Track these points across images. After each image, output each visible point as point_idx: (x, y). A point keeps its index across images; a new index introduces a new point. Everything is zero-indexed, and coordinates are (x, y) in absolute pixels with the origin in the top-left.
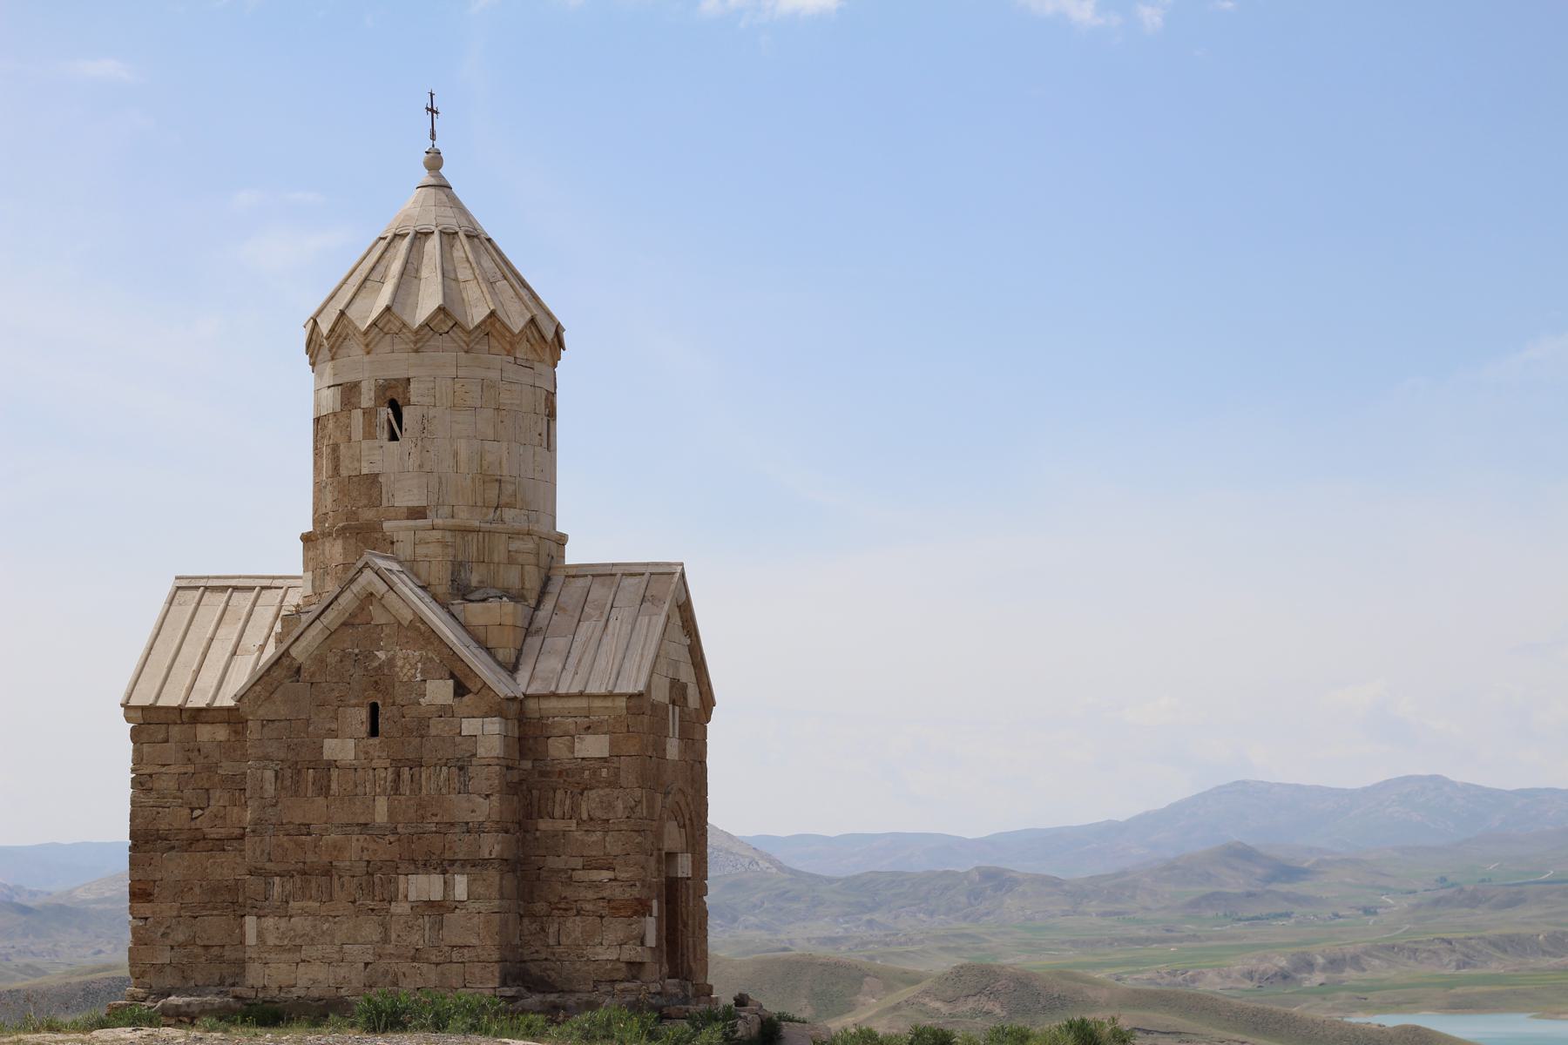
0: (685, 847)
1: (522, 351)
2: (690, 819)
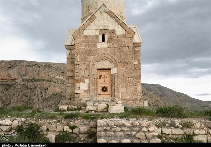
0: (114, 67)
2: (115, 60)
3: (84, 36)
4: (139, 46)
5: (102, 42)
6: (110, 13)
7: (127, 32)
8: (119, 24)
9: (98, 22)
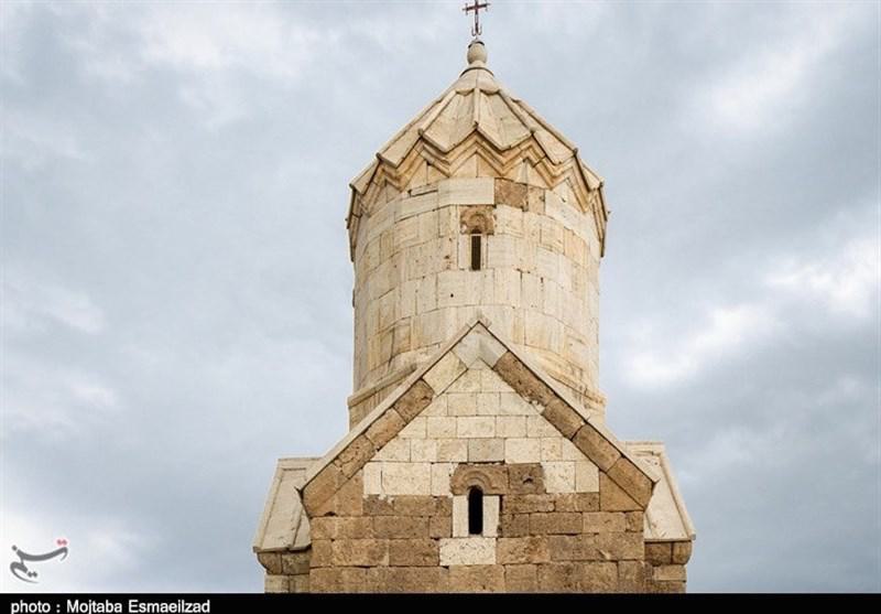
1: (419, 178)
3: (365, 497)
4: (675, 560)
5: (467, 534)
6: (513, 372)
7: (610, 478)
8: (565, 436)
9: (449, 424)
